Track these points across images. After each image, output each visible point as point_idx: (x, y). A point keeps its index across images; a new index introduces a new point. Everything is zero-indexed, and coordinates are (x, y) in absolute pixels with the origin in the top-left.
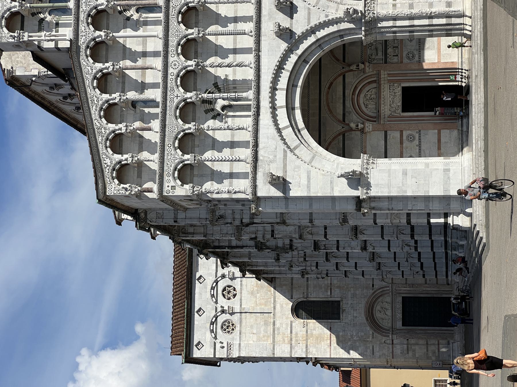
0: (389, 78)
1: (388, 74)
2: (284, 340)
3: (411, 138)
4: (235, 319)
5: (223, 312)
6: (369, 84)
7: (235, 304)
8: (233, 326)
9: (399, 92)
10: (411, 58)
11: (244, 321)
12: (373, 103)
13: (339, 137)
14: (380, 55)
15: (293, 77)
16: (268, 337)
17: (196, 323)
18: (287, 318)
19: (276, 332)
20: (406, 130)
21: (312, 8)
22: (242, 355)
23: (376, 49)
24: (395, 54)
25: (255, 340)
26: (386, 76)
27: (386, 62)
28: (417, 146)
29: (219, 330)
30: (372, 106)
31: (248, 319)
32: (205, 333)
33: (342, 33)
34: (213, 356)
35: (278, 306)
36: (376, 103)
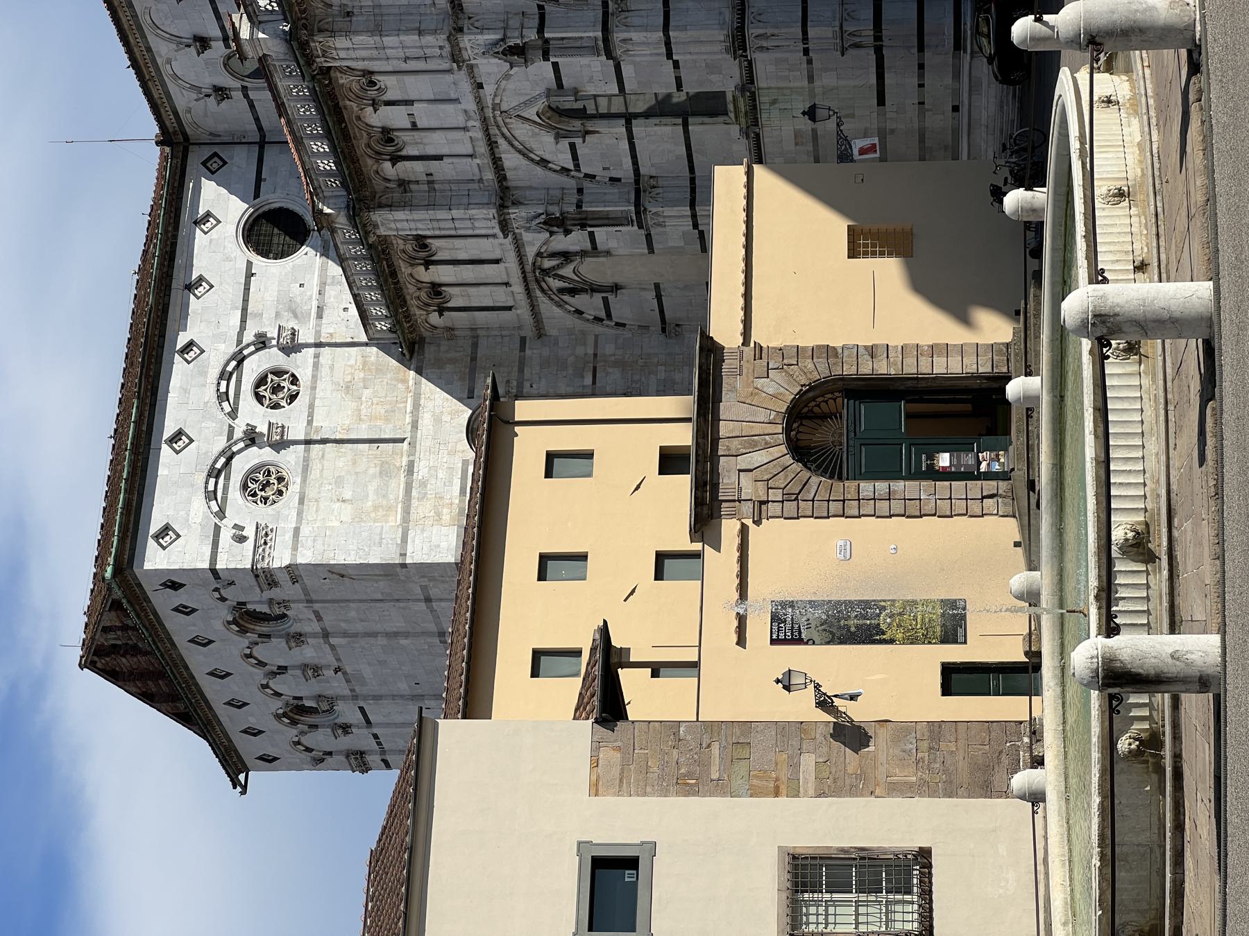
2: (439, 515)
4: (289, 459)
5: (252, 438)
7: (294, 420)
8: (279, 484)
11: (315, 467)
16: (389, 508)
17: (162, 471)
18: (452, 453)
19: (414, 493)
22: (301, 560)
25: (346, 517)
29: (235, 494)
31: (330, 460)
32: (189, 501)
34: (206, 565)
35: (426, 421)
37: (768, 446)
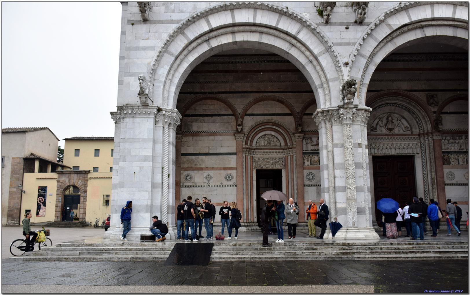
0: (289, 157)
1: (293, 156)
3: (229, 177)
6: (283, 139)
9: (277, 167)
10: (309, 178)
12: (266, 143)
13: (231, 111)
14: (310, 148)
15: (271, 31)
20: (237, 173)
21: (356, 47)
24: (312, 162)
26: (291, 154)
27: (304, 153)
28: (222, 183)
30: (263, 142)
33: (325, 86)
36: (266, 146)
37: (69, 182)
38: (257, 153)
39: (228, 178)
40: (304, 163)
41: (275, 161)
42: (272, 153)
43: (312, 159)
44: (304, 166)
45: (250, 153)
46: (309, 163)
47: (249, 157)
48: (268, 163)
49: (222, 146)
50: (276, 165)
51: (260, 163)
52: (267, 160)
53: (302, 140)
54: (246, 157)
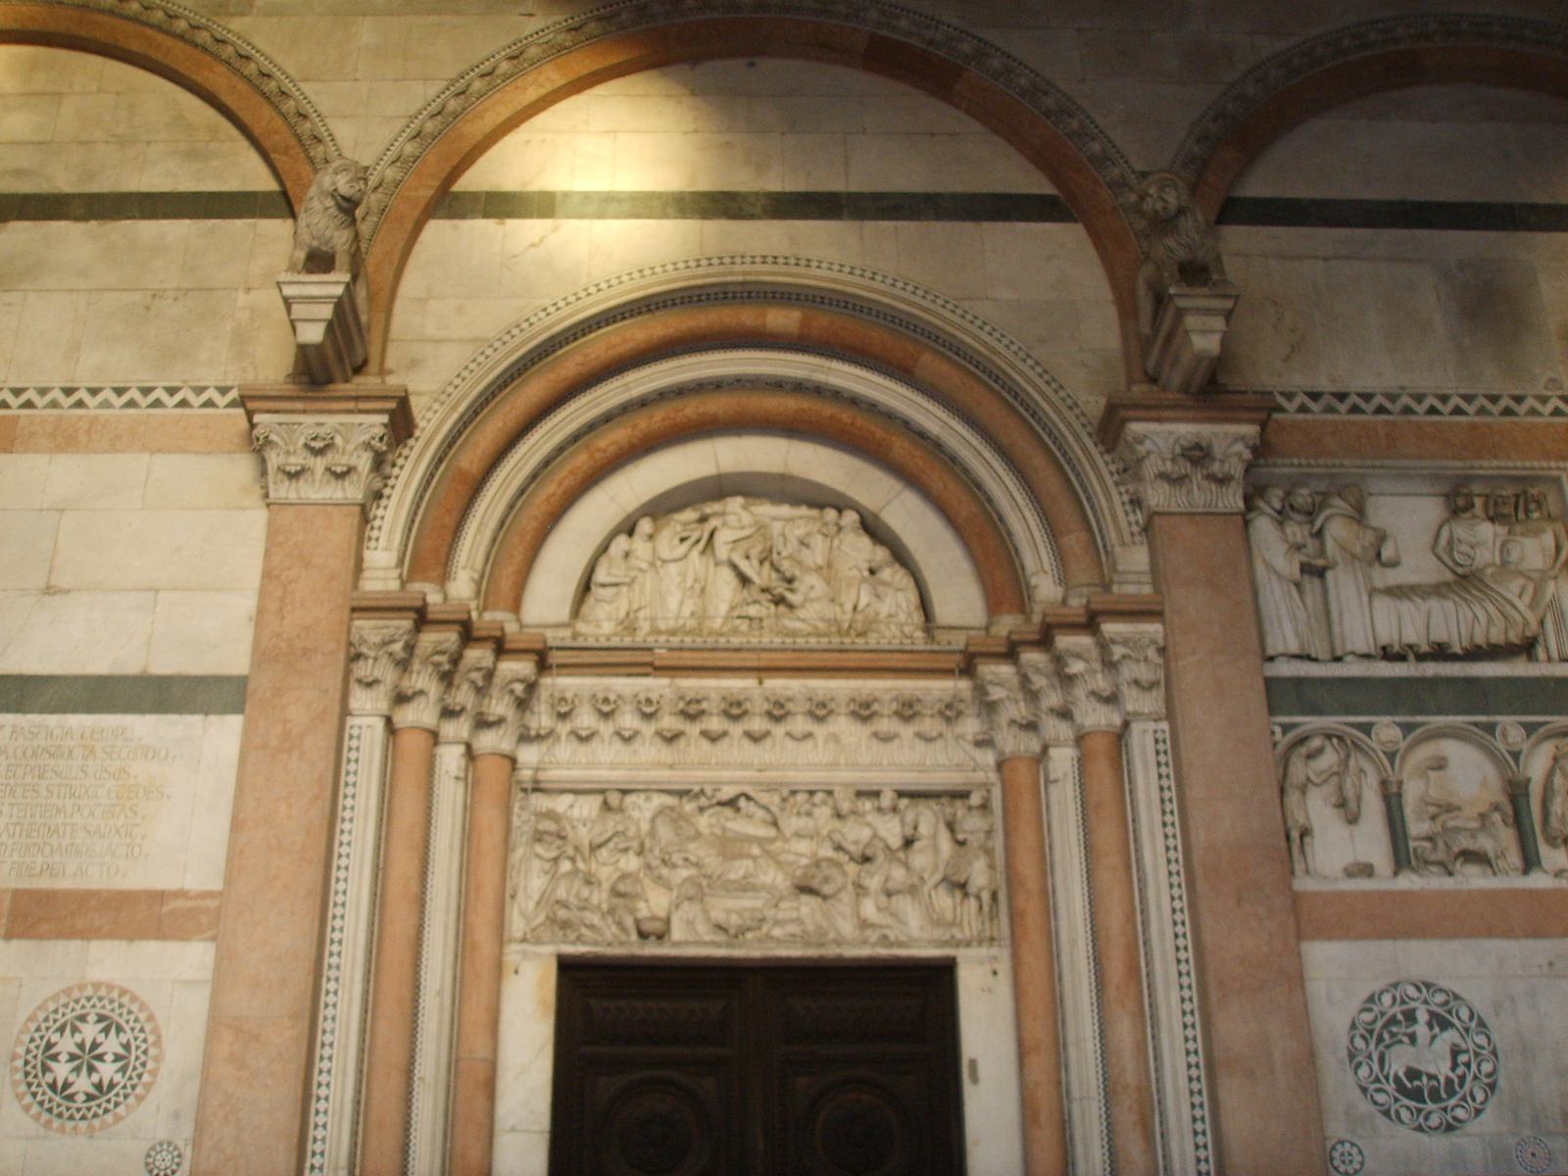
1: (1120, 737)
3: (87, 1057)
10: (1397, 1066)
23: (1465, 581)
24: (1416, 827)
26: (1095, 717)
38: (585, 719)
39: (62, 1070)
40: (1293, 840)
41: (856, 834)
42: (800, 724)
43: (1412, 792)
44: (1302, 884)
45: (463, 696)
46: (1371, 842)
47: (450, 758)
48: (739, 869)
49: (61, 580)
50: (860, 889)
51: (631, 863)
52: (738, 825)
53: (1232, 499)
54: (412, 745)
